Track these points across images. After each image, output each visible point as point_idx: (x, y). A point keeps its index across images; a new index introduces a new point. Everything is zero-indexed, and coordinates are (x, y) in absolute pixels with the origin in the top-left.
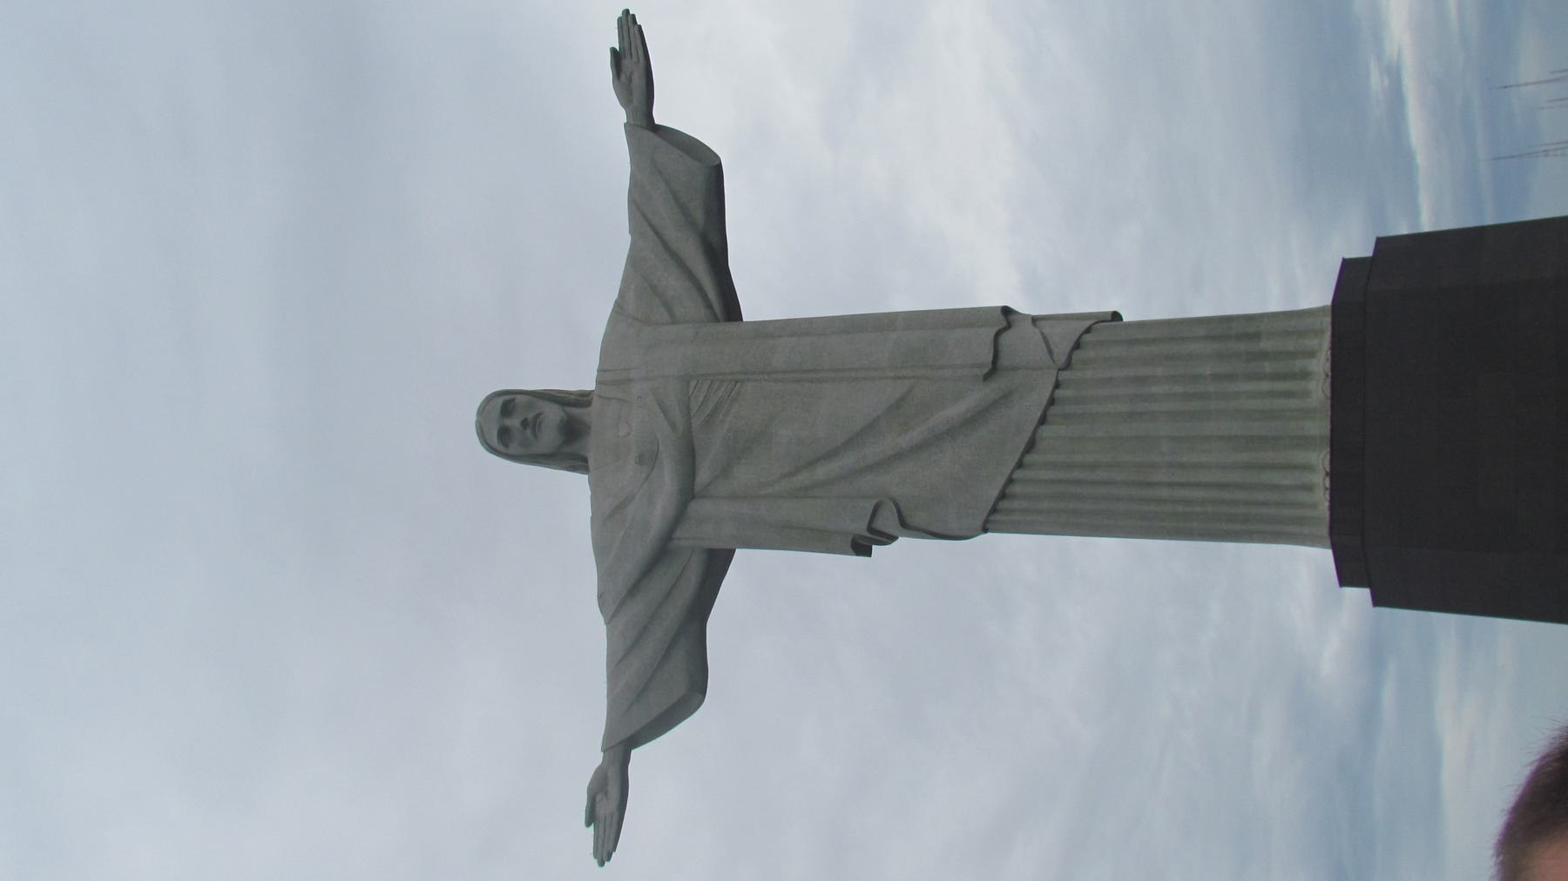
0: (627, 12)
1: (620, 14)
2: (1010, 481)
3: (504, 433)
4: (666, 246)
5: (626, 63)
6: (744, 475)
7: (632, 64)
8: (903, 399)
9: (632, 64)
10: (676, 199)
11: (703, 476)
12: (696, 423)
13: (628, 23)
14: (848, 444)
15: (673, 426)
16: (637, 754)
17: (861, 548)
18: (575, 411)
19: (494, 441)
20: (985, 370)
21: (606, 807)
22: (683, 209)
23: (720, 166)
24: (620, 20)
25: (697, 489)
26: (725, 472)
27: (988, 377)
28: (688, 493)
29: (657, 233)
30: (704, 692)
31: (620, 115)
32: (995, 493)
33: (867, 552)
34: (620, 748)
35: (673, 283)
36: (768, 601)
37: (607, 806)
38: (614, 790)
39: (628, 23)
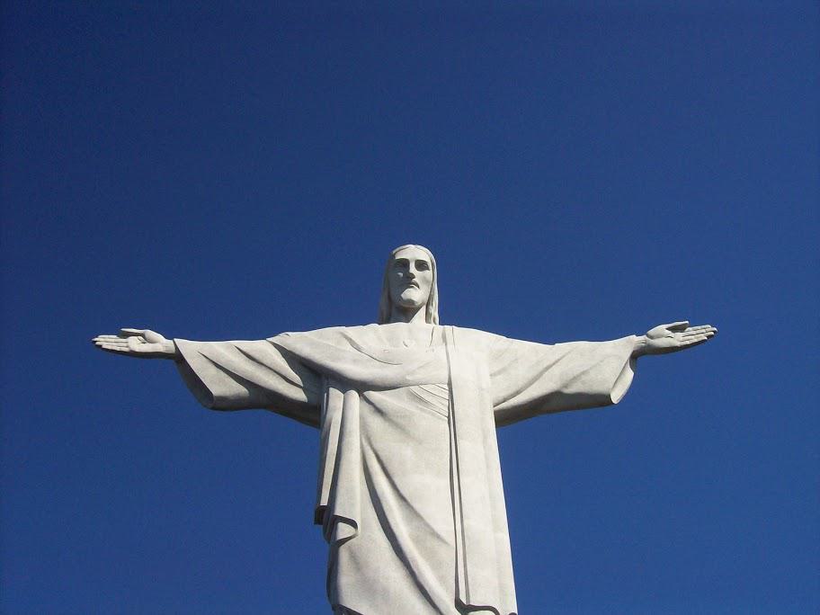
3: (405, 263)
4: (547, 368)
5: (679, 335)
6: (376, 422)
8: (438, 537)
10: (583, 373)
11: (374, 396)
12: (414, 389)
14: (401, 497)
15: (412, 373)
18: (422, 312)
19: (398, 257)
20: (465, 602)
21: (135, 344)
22: (575, 379)
25: (365, 393)
26: (379, 411)
27: (458, 604)
28: (362, 387)
29: (557, 362)
30: (213, 408)
33: (319, 520)
35: (520, 374)
38: (147, 348)
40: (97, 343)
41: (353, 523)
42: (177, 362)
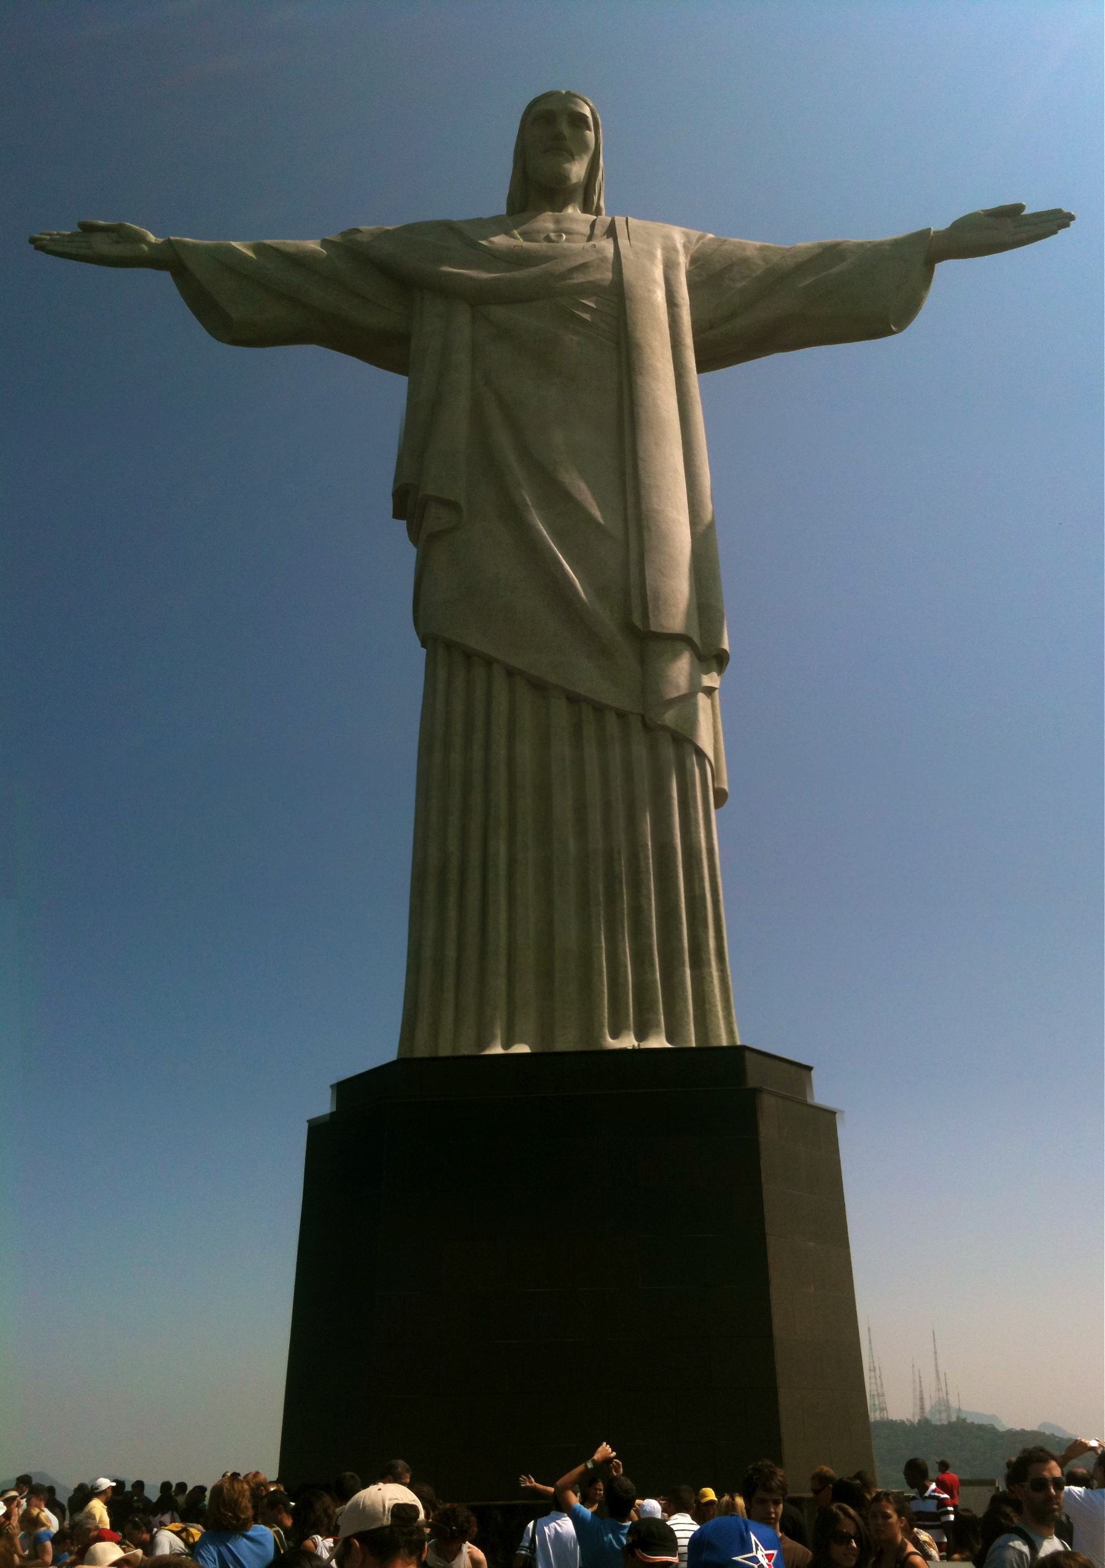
0: (1072, 218)
1: (1065, 210)
2: (489, 662)
7: (1004, 229)
9: (1004, 229)
13: (1055, 221)
16: (166, 277)
17: (408, 503)
23: (886, 332)
24: (1059, 211)
31: (940, 222)
32: (474, 640)
34: (171, 260)
36: (350, 412)
37: (102, 247)
39: (1055, 221)
40: (39, 243)
41: (454, 506)
42: (175, 275)
